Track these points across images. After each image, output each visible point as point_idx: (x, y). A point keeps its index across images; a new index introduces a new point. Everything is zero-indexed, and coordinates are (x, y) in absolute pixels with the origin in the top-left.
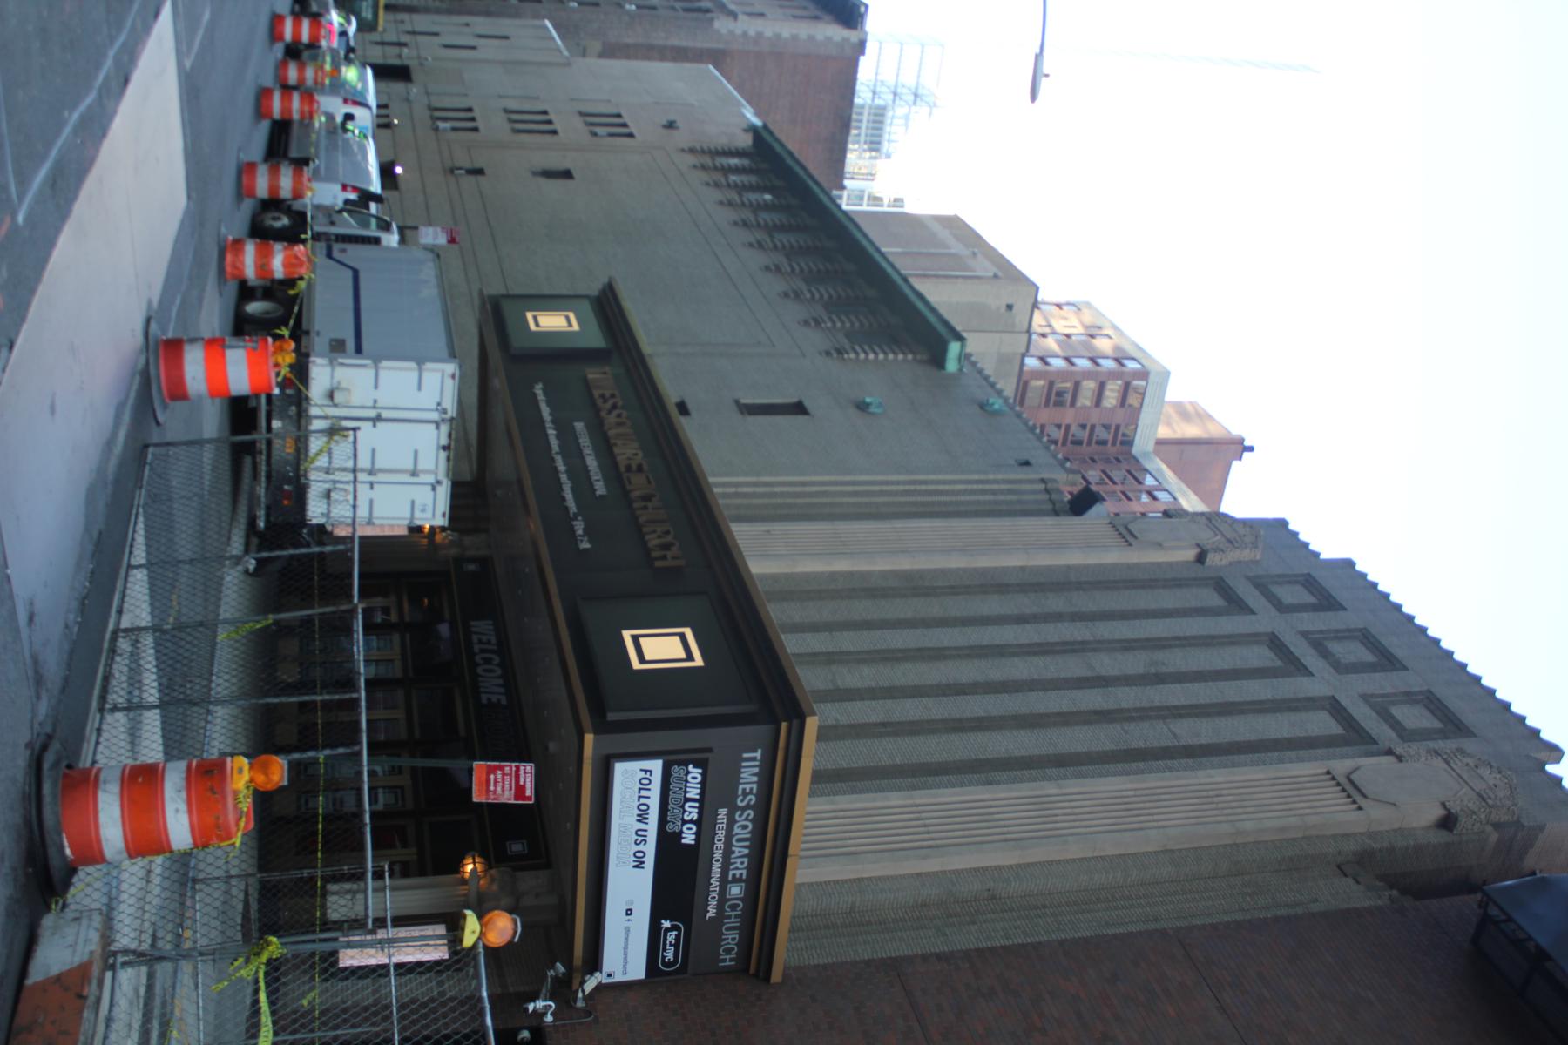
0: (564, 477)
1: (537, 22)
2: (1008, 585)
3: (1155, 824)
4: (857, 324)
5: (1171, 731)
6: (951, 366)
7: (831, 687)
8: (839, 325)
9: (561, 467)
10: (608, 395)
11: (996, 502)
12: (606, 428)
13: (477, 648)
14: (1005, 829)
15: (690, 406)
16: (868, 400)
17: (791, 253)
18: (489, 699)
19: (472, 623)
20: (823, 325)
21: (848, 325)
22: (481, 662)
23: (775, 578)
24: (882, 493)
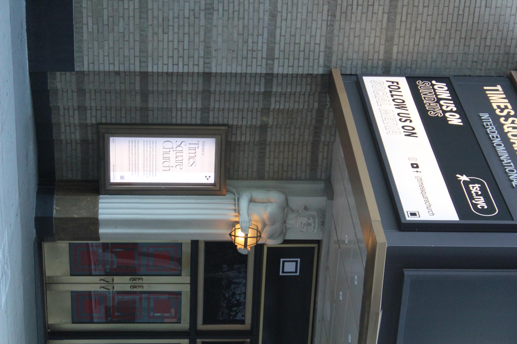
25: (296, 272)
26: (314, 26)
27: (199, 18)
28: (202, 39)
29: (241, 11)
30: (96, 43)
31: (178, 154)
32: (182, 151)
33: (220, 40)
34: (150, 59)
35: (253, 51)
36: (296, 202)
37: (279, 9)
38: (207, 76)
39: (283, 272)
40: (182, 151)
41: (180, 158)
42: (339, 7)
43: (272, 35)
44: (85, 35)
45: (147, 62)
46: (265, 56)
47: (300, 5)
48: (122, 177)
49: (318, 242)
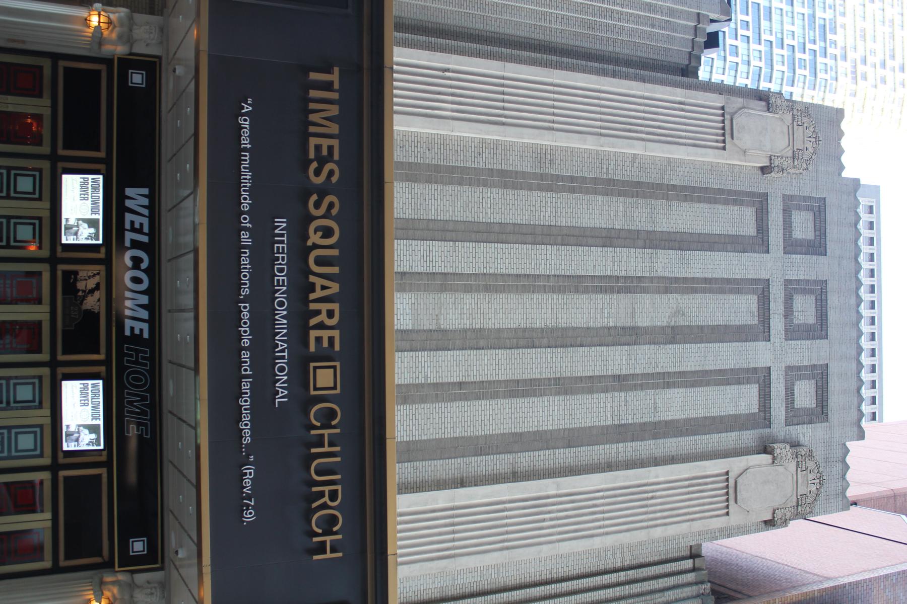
0: (245, 356)
2: (614, 182)
3: (602, 530)
5: (655, 403)
7: (434, 327)
9: (246, 342)
10: (325, 152)
11: (650, 35)
12: (309, 243)
13: (129, 236)
14: (505, 537)
18: (132, 329)
19: (129, 192)
22: (129, 263)
23: (430, 142)
25: (142, 74)
36: (140, 18)
49: (160, 58)
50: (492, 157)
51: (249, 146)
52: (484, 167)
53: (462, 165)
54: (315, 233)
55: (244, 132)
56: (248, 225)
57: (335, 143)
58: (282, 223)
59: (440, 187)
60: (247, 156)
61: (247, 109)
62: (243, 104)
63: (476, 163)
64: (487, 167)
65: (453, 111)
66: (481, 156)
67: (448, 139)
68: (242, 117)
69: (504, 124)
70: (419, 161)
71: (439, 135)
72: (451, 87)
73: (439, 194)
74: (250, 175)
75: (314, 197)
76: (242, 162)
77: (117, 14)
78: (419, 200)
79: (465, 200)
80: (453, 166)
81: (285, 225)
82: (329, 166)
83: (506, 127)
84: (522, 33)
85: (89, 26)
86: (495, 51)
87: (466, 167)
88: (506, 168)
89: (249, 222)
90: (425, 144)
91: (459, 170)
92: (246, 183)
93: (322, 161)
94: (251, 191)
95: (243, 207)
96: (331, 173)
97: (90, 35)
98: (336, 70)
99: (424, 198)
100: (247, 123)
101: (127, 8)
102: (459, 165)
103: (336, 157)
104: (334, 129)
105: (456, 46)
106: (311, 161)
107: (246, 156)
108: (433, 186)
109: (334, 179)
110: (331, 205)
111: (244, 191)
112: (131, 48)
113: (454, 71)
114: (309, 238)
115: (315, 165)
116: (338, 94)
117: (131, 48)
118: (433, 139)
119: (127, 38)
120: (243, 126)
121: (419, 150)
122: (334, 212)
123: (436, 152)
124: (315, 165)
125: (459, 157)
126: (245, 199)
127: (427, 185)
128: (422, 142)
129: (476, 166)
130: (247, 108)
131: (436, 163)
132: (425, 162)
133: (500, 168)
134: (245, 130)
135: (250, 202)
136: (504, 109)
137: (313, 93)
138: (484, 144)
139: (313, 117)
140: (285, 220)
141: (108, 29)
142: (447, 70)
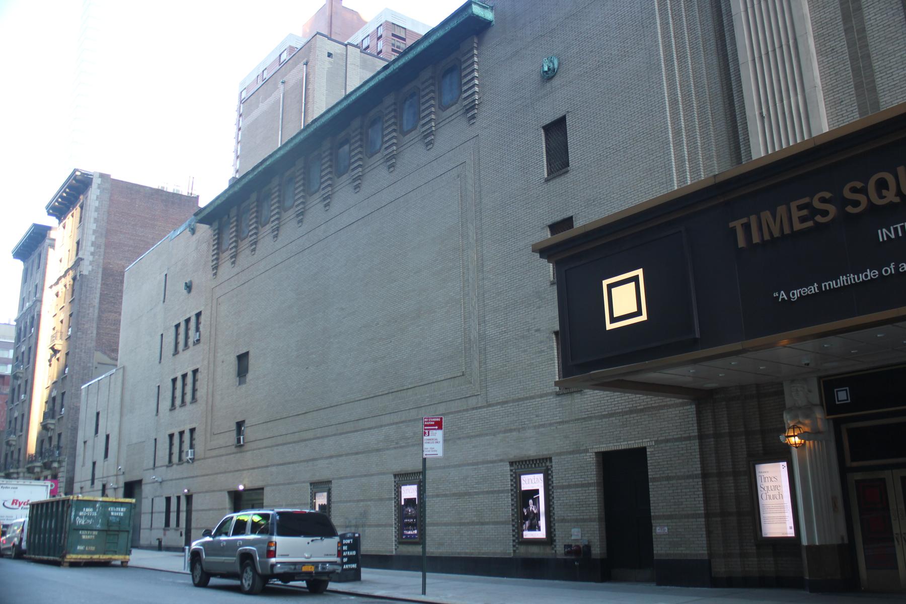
1: (83, 393)
4: (432, 102)
6: (489, 15)
8: (433, 116)
10: (804, 212)
12: (897, 200)
15: (558, 217)
16: (546, 69)
17: (261, 223)
20: (433, 129)
21: (433, 109)
23: (833, 104)
24: (679, 36)
26: (670, 416)
27: (673, 484)
28: (683, 481)
29: (667, 459)
30: (691, 546)
31: (770, 489)
32: (768, 487)
33: (683, 470)
34: (697, 512)
35: (687, 450)
36: (788, 402)
37: (664, 438)
38: (705, 476)
39: (847, 400)
40: (768, 487)
41: (772, 487)
42: (660, 404)
43: (676, 440)
44: (688, 552)
45: (699, 514)
46: (688, 442)
47: (661, 426)
48: (791, 528)
49: (819, 378)
50: (832, 36)
51: (816, 285)
52: (845, 40)
53: (849, 62)
54: (885, 197)
55: (804, 293)
56: (892, 266)
57: (794, 205)
58: (883, 234)
59: (878, 75)
60: (825, 285)
61: (783, 295)
62: (780, 300)
63: (843, 49)
64: (844, 37)
65: (796, 94)
66: (834, 47)
67: (827, 87)
68: (791, 298)
69: (795, 40)
70: (856, 107)
71: (825, 97)
72: (775, 105)
73: (884, 74)
74: (843, 278)
75: (850, 209)
76: (832, 287)
77: (789, 421)
78: (897, 91)
79: (885, 44)
80: (853, 71)
81: (884, 230)
82: (817, 204)
83: (798, 35)
84: (714, 60)
85: (804, 445)
86: (735, 78)
87: (850, 57)
88: (840, 17)
89: (889, 266)
90: (837, 108)
91: (855, 63)
92: (850, 279)
93: (815, 212)
94: (857, 273)
95: (874, 276)
96: (823, 200)
97: (811, 442)
98: (732, 225)
99: (893, 86)
100: (795, 292)
101: (783, 414)
102: (850, 65)
103: (806, 200)
104: (781, 210)
105: (740, 115)
106: (816, 223)
107: (825, 285)
108: (878, 83)
109: (827, 195)
110: (854, 190)
111: (859, 279)
112: (816, 405)
113: (761, 108)
114: (891, 201)
115: (819, 219)
116: (751, 217)
117: (816, 405)
118: (831, 102)
119: (807, 410)
120: (799, 296)
121: (845, 112)
122: (859, 185)
123: (842, 94)
124: (819, 219)
125: (841, 69)
126: (866, 276)
127: (878, 89)
128: (837, 112)
129: (846, 48)
130: (783, 295)
131: (853, 89)
132: (855, 101)
133: (841, 23)
134: (802, 292)
135: (868, 270)
136: (781, 47)
137: (756, 239)
138: (822, 50)
139: (776, 234)
140: (879, 231)
141: (799, 428)
142: (761, 114)
